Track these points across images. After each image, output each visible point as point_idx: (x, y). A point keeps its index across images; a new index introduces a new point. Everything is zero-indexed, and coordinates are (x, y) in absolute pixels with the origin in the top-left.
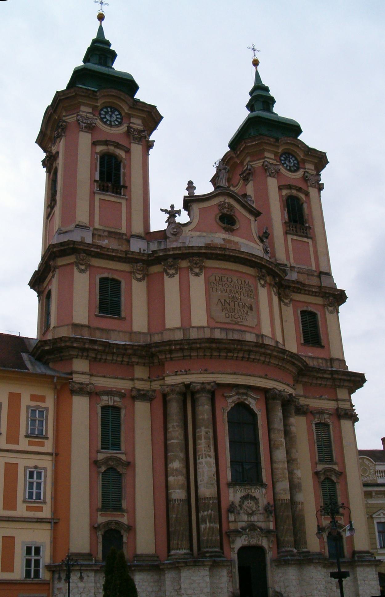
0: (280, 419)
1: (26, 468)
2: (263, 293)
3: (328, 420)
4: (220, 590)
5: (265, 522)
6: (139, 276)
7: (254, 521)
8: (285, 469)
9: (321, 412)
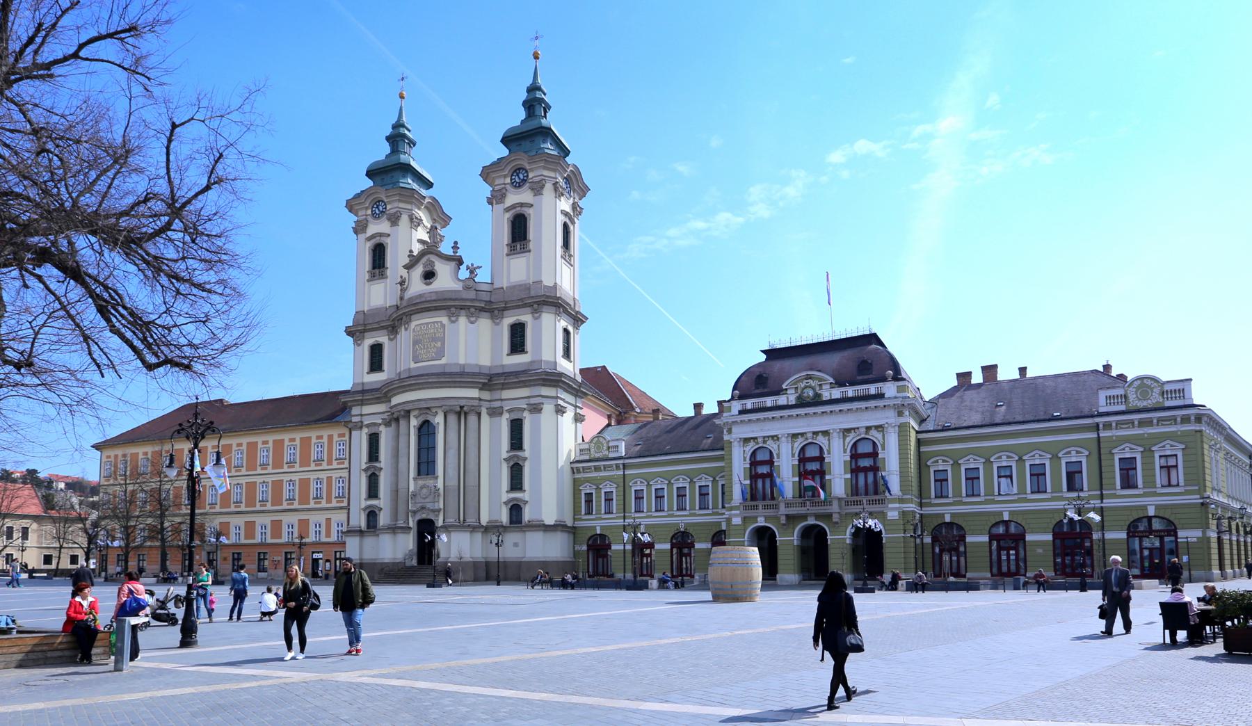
1: (336, 478)
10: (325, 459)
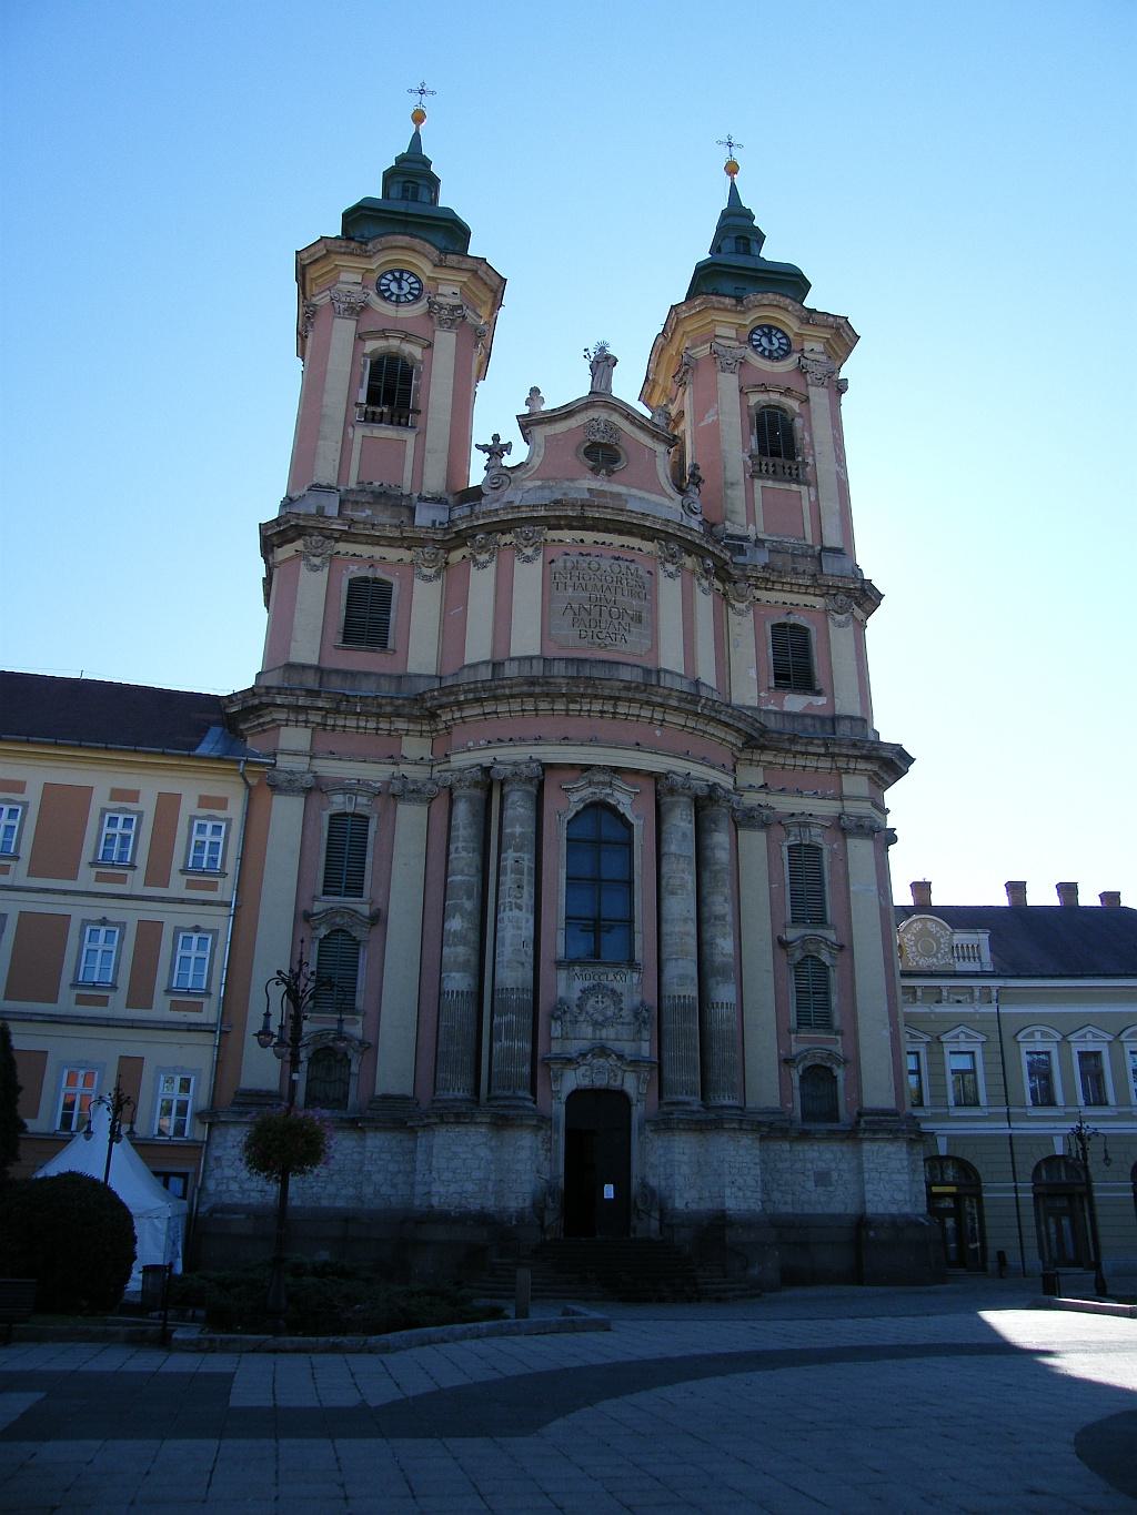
0: (684, 835)
1: (178, 930)
2: (670, 592)
3: (820, 840)
4: (514, 1176)
5: (634, 1040)
6: (427, 571)
7: (607, 1039)
8: (688, 934)
9: (804, 820)
10: (142, 860)
